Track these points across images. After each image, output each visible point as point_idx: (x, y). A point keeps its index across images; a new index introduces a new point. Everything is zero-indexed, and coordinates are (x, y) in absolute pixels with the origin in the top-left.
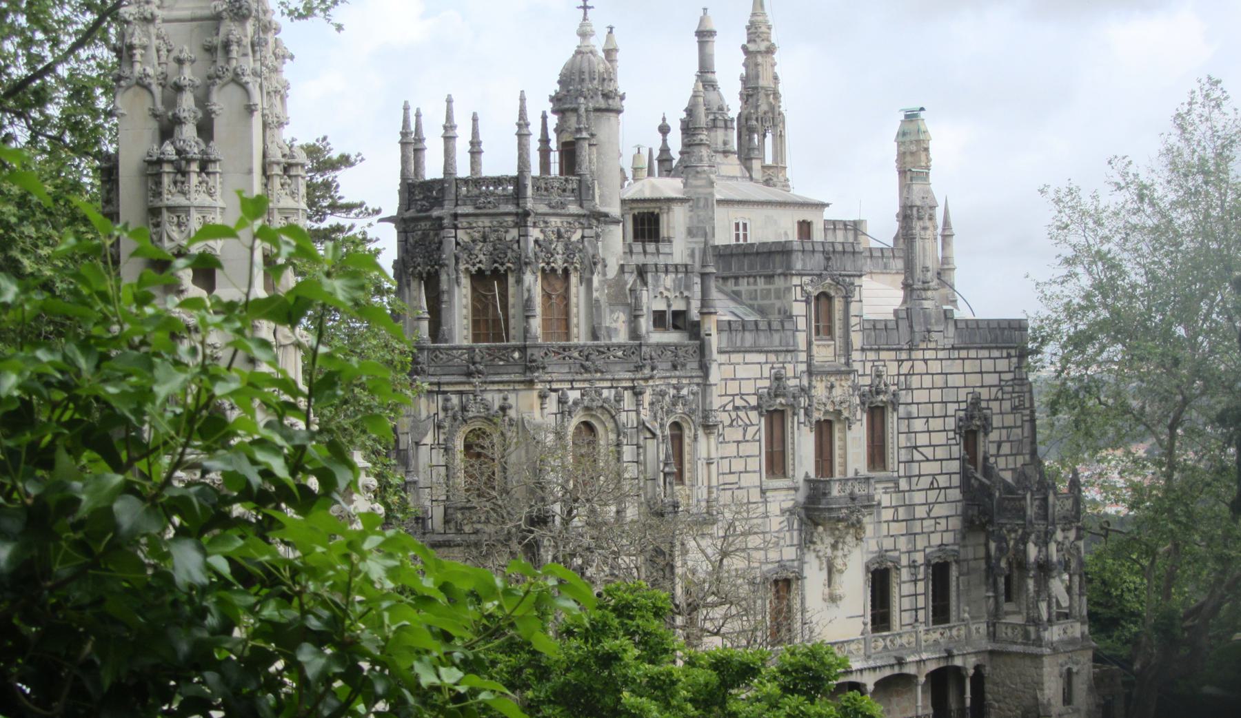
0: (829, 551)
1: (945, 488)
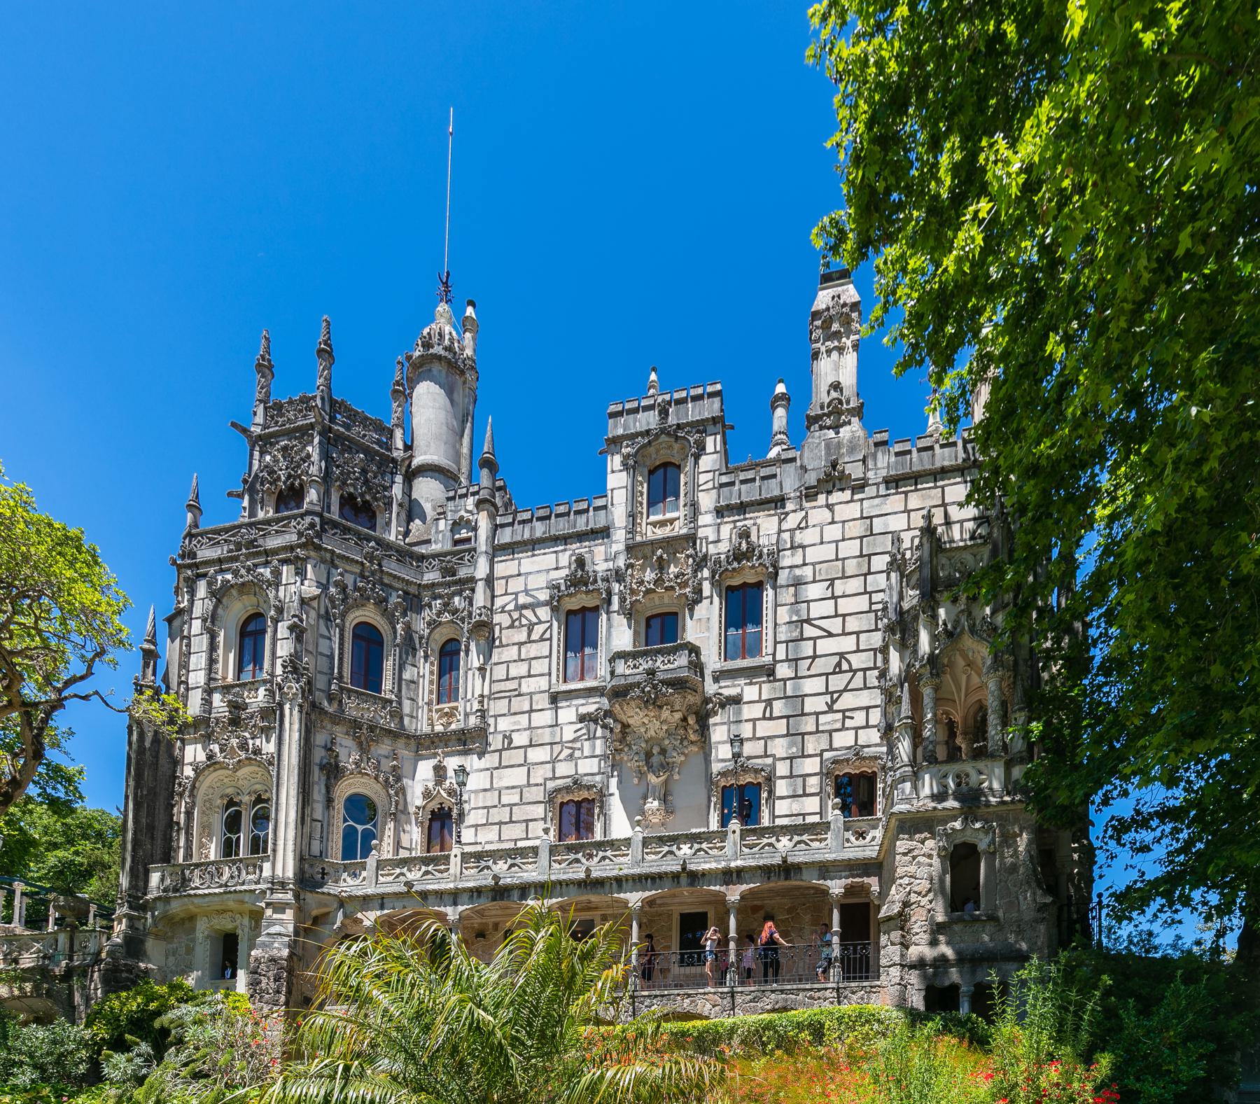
1: (864, 670)
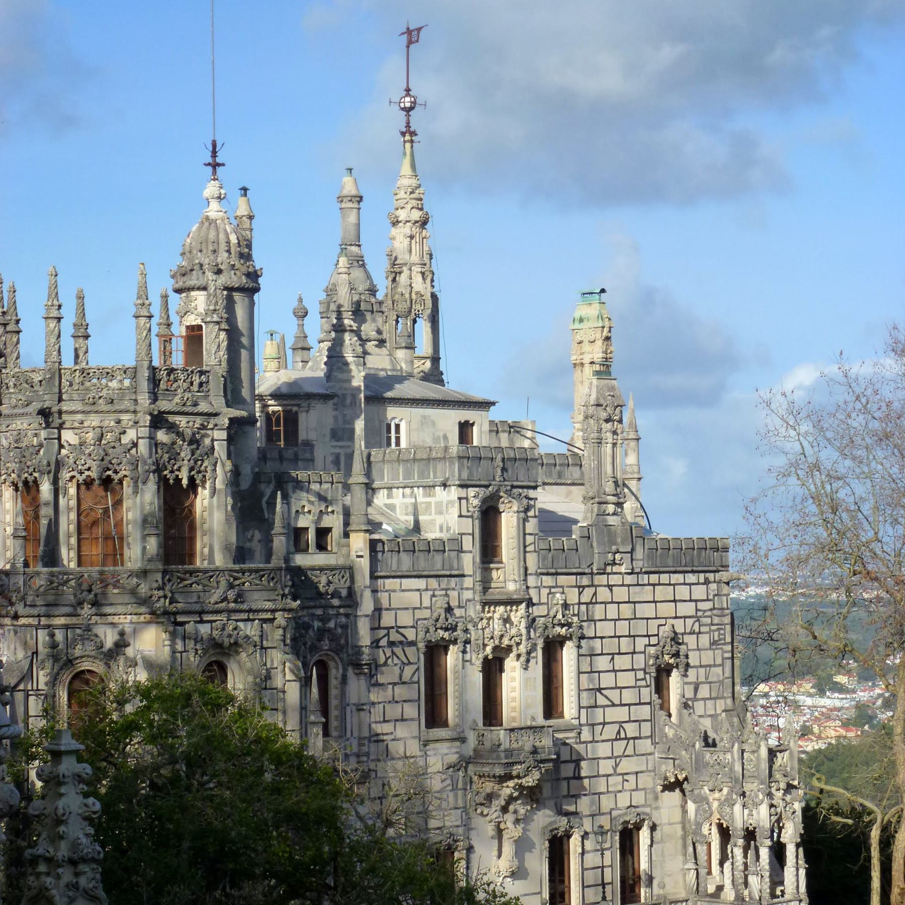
1: (634, 738)
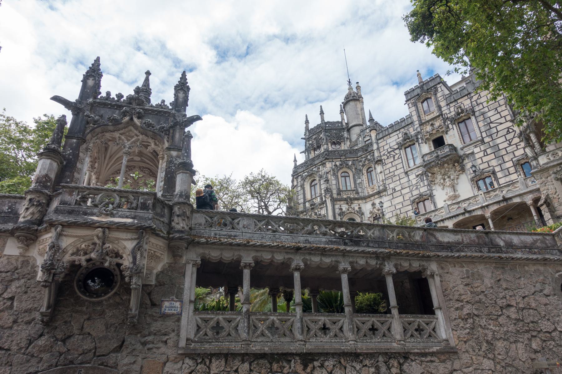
0: (442, 181)
